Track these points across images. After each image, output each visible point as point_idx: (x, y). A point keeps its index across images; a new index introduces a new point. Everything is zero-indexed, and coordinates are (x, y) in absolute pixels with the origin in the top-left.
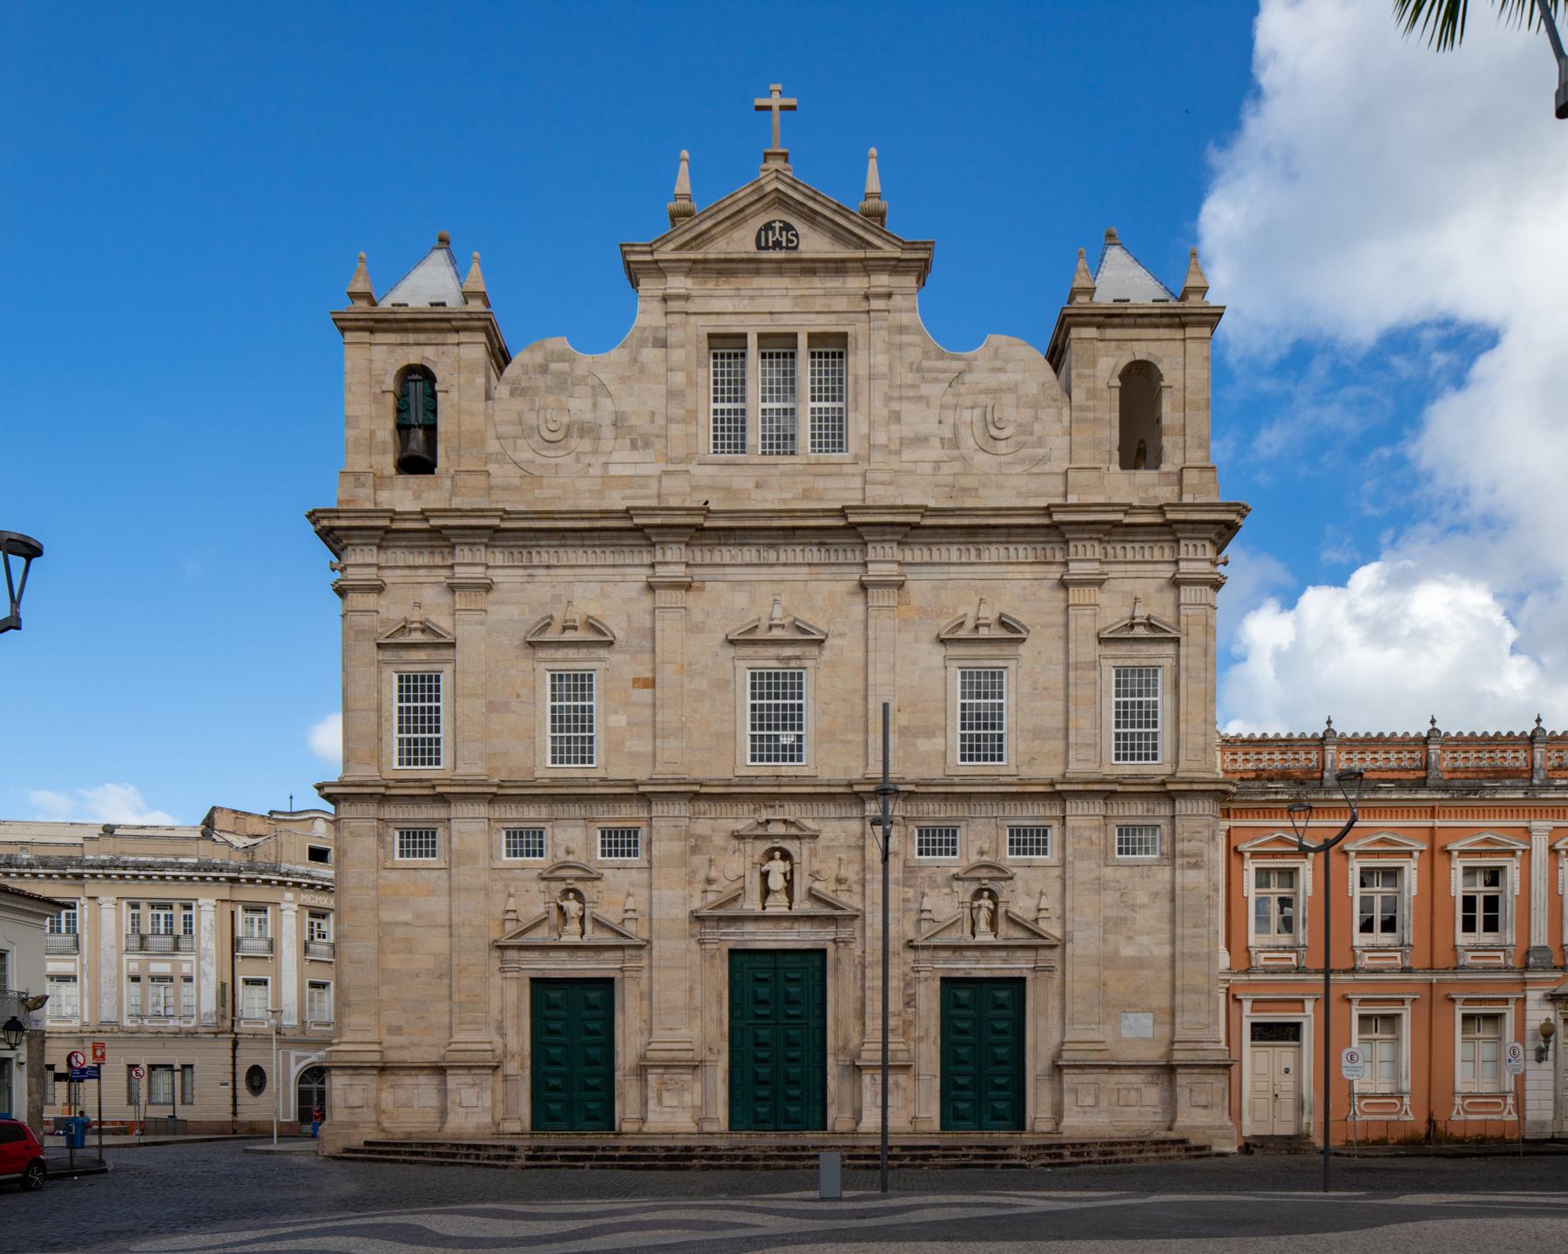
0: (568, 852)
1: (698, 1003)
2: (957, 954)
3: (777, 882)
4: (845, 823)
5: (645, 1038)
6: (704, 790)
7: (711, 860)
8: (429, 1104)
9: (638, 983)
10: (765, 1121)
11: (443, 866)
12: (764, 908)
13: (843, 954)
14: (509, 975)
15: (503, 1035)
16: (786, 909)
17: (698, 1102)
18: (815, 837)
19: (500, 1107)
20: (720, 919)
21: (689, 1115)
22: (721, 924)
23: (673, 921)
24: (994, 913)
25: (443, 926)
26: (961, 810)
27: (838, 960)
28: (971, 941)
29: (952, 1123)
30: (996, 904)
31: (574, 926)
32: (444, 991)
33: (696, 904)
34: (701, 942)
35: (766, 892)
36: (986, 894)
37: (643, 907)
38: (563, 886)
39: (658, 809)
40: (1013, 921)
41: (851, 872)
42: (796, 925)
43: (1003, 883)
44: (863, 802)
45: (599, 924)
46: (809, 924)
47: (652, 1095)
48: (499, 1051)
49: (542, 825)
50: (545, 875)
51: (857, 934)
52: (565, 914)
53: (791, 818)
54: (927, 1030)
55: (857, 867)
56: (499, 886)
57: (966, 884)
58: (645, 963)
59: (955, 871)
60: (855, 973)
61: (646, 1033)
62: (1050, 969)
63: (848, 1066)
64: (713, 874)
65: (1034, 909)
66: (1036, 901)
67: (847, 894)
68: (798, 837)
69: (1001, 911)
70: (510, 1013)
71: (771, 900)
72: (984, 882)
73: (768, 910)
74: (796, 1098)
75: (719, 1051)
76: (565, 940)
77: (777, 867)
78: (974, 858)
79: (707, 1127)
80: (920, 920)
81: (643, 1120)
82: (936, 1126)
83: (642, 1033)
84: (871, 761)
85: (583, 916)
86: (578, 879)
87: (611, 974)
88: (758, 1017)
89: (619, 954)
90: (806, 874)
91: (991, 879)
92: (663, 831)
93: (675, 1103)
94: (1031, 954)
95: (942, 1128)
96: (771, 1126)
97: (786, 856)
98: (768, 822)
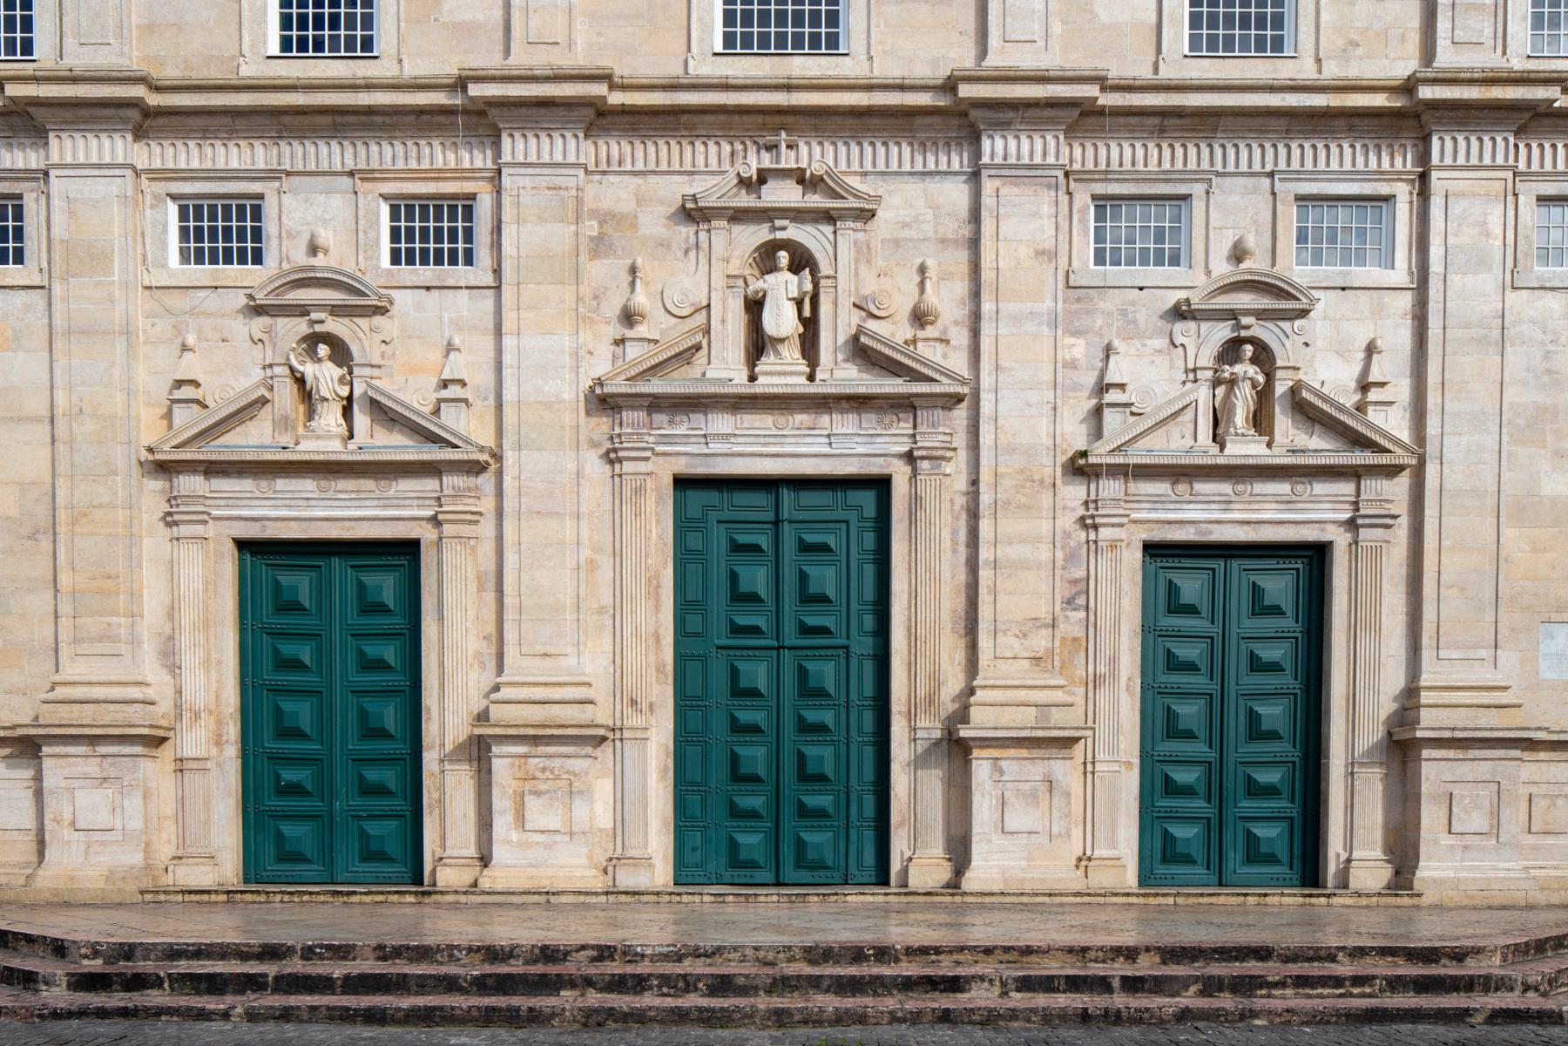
0: (314, 249)
1: (607, 600)
2: (1182, 488)
3: (781, 320)
4: (934, 185)
5: (489, 678)
6: (616, 98)
7: (633, 270)
8: (13, 822)
9: (473, 549)
10: (753, 865)
11: (37, 281)
12: (752, 378)
13: (926, 486)
14: (184, 530)
15: (174, 668)
16: (803, 380)
17: (604, 819)
18: (866, 215)
19: (170, 830)
20: (656, 404)
21: (584, 850)
22: (661, 418)
23: (549, 406)
24: (1264, 395)
25: (38, 420)
26: (1191, 155)
27: (915, 500)
28: (1213, 456)
29: (1161, 870)
30: (1270, 378)
31: (330, 418)
32: (43, 569)
33: (600, 365)
34: (611, 458)
35: (758, 344)
36: (1248, 350)
37: (480, 378)
38: (301, 327)
39: (514, 147)
40: (1307, 412)
41: (947, 299)
42: (825, 419)
43: (1286, 325)
44: (973, 138)
45: (384, 414)
46: (852, 418)
47: (501, 803)
48: (165, 706)
49: (255, 187)
50: (261, 298)
51: (960, 440)
52: (310, 394)
53: (817, 168)
54: (1114, 661)
55: (961, 287)
56: (164, 326)
57: (1204, 326)
58: (487, 505)
59: (1182, 295)
60: (954, 532)
61: (492, 665)
62: (1385, 521)
63: (938, 743)
64: (641, 299)
65: (1353, 385)
66: (1357, 368)
67: (940, 347)
68: (829, 217)
69: (1281, 388)
70: (187, 618)
71: (767, 363)
72: (1245, 321)
73: (761, 380)
74: (821, 813)
75: (651, 706)
76: (309, 449)
77: (783, 287)
78: (1222, 268)
79: (627, 880)
80: (1098, 412)
81: (485, 860)
82: (1131, 878)
83: (482, 665)
84: (994, 41)
85: (350, 398)
86: (336, 310)
87: (413, 535)
88: (737, 630)
89: (429, 485)
90: (845, 303)
91: (1262, 315)
92: (526, 198)
93: (554, 822)
94: (1346, 488)
95: (1141, 884)
96: (768, 876)
97: (802, 261)
98: (763, 177)
